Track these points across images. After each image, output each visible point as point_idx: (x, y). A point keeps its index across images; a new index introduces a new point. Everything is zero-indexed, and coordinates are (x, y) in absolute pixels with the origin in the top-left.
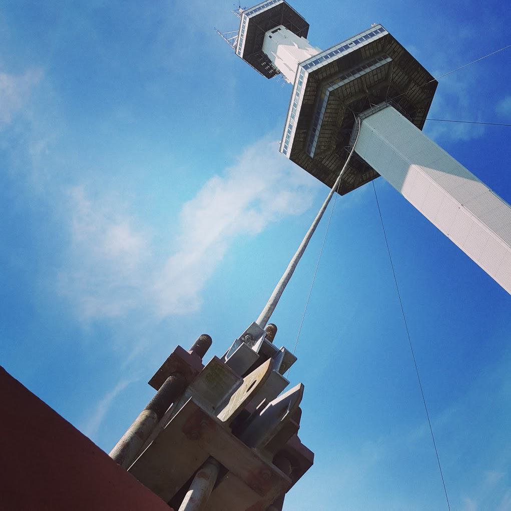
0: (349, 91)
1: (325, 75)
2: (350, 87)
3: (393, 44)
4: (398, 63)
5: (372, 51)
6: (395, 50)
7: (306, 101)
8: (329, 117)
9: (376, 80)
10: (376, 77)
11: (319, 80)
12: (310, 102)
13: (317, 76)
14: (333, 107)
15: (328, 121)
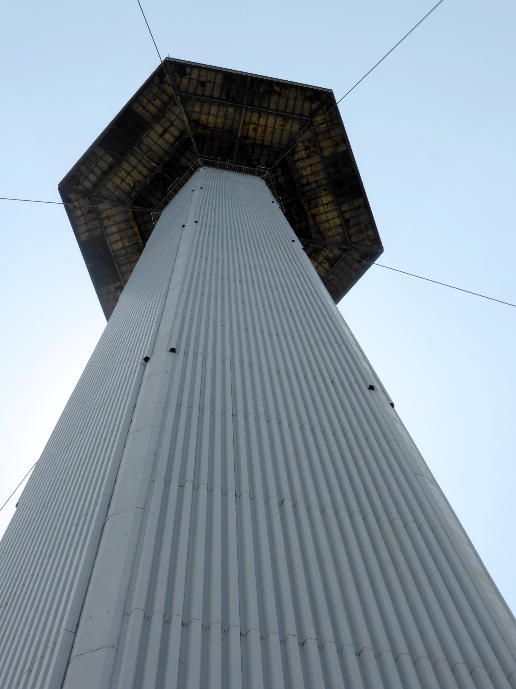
0: (129, 180)
1: (93, 178)
2: (129, 174)
3: (190, 74)
4: (223, 96)
5: (157, 103)
6: (203, 79)
7: (87, 234)
8: (122, 239)
9: (172, 140)
10: (167, 136)
11: (87, 190)
12: (97, 233)
13: (80, 187)
14: (118, 218)
15: (124, 248)
